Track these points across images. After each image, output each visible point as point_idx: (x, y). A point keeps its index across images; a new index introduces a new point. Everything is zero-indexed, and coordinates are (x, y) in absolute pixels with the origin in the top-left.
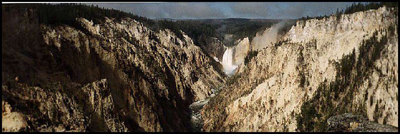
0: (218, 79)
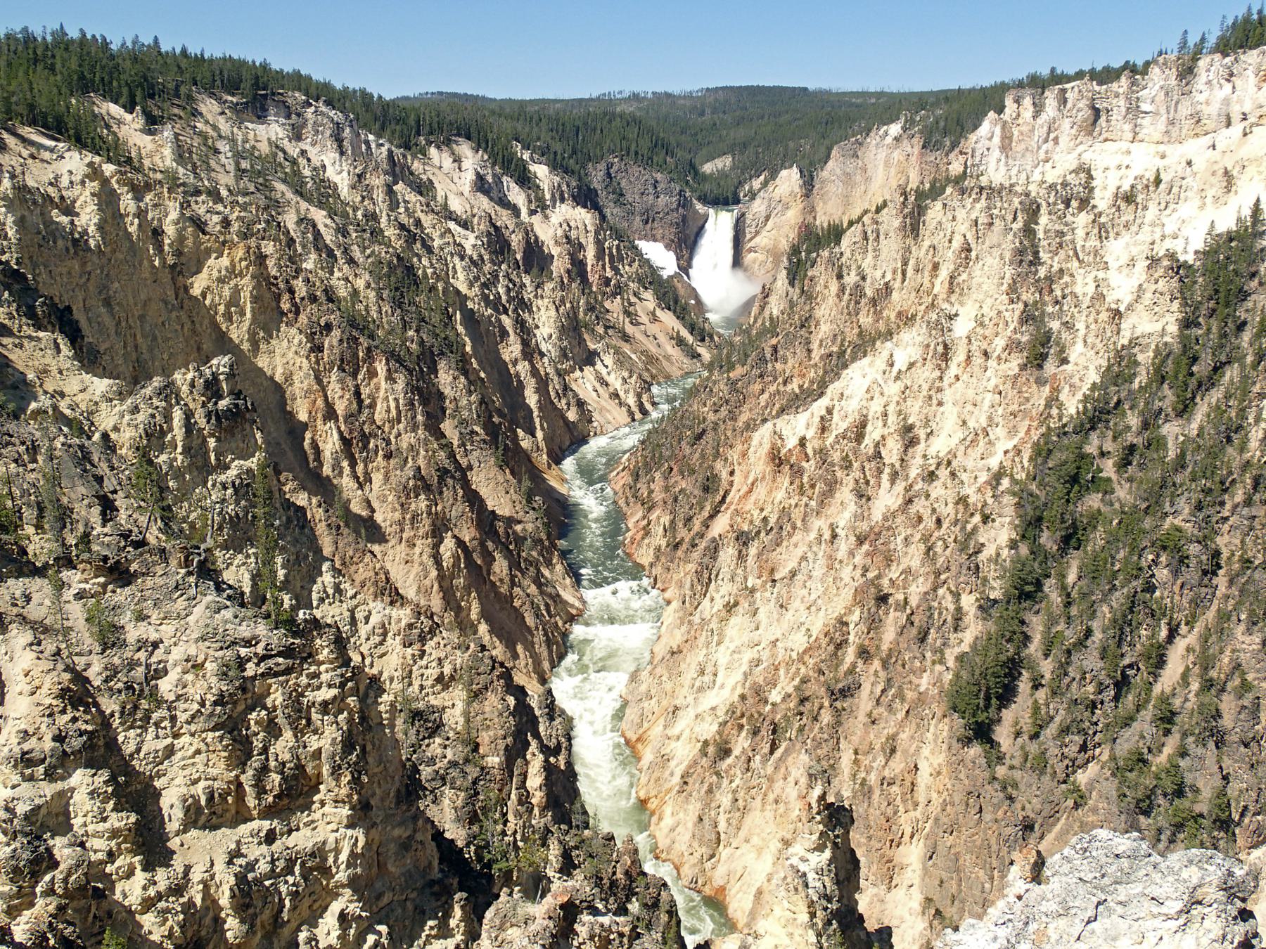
0: (680, 342)
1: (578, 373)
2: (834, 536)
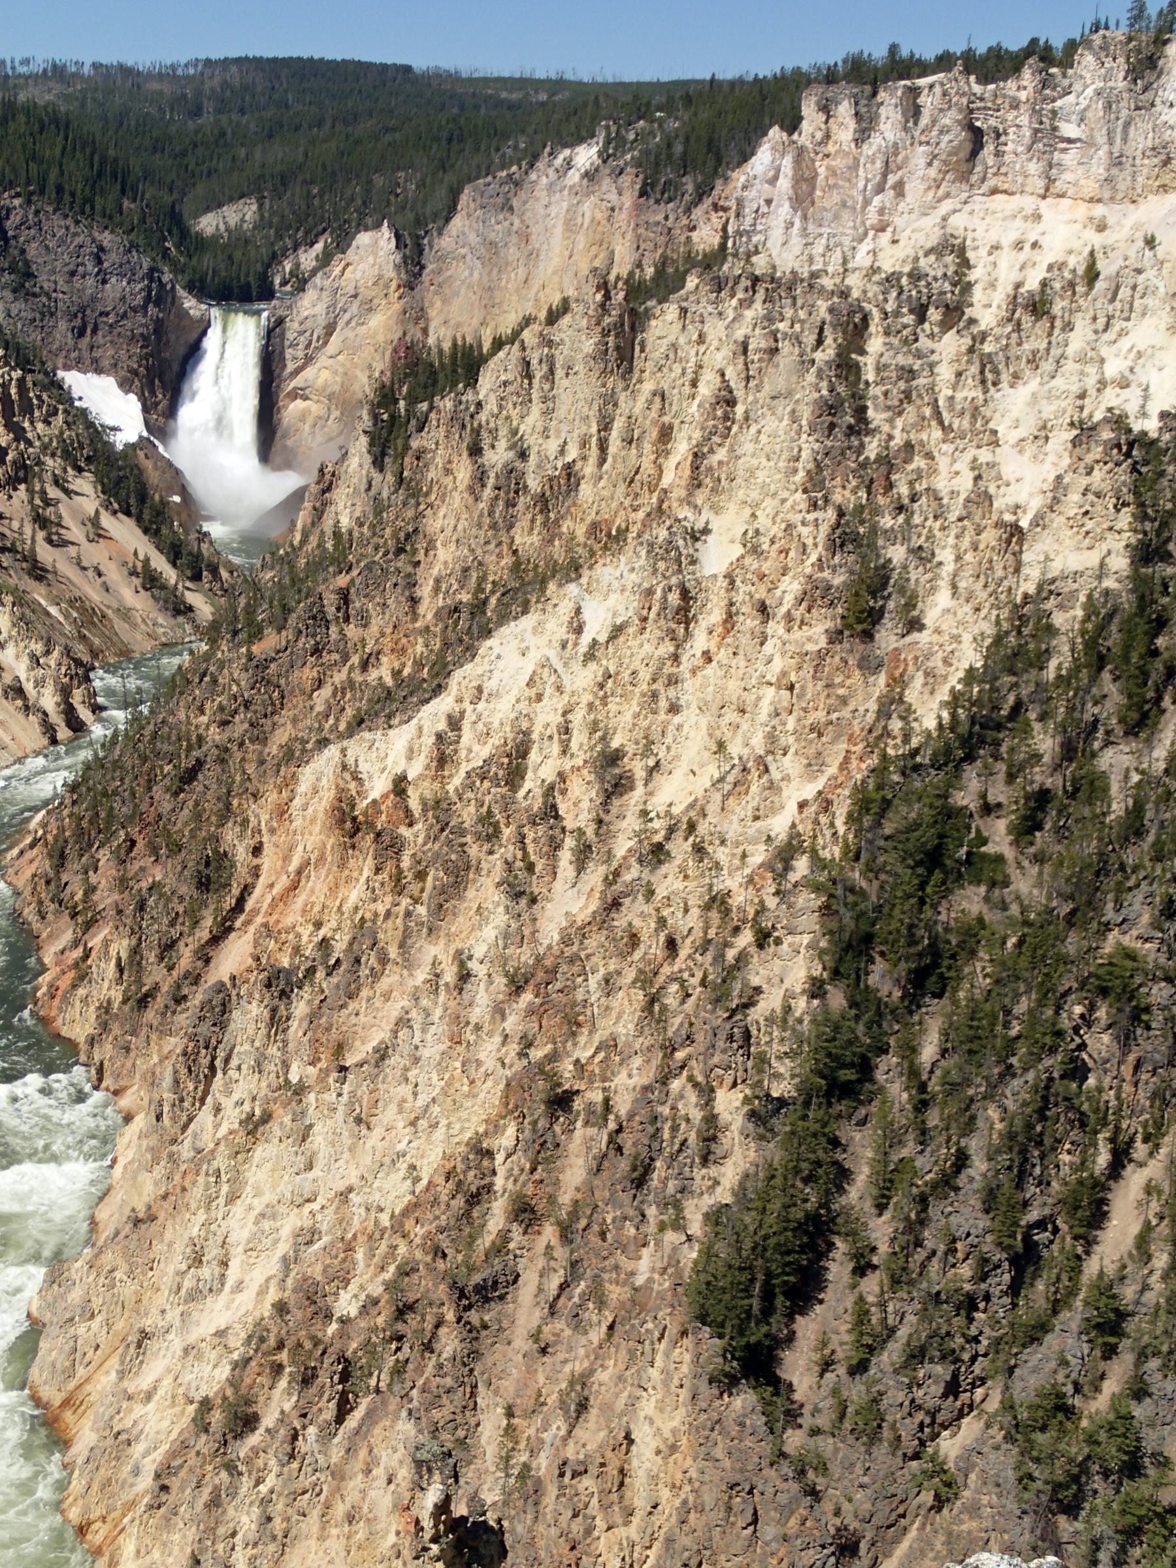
0: (151, 581)
2: (465, 976)
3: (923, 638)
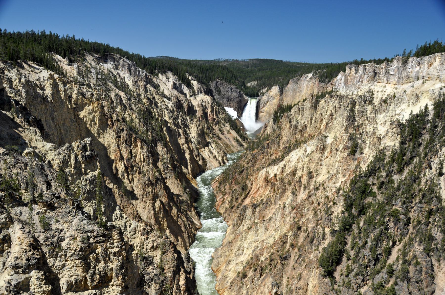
0: (237, 141)
1: (203, 149)
2: (284, 207)
3: (363, 155)
